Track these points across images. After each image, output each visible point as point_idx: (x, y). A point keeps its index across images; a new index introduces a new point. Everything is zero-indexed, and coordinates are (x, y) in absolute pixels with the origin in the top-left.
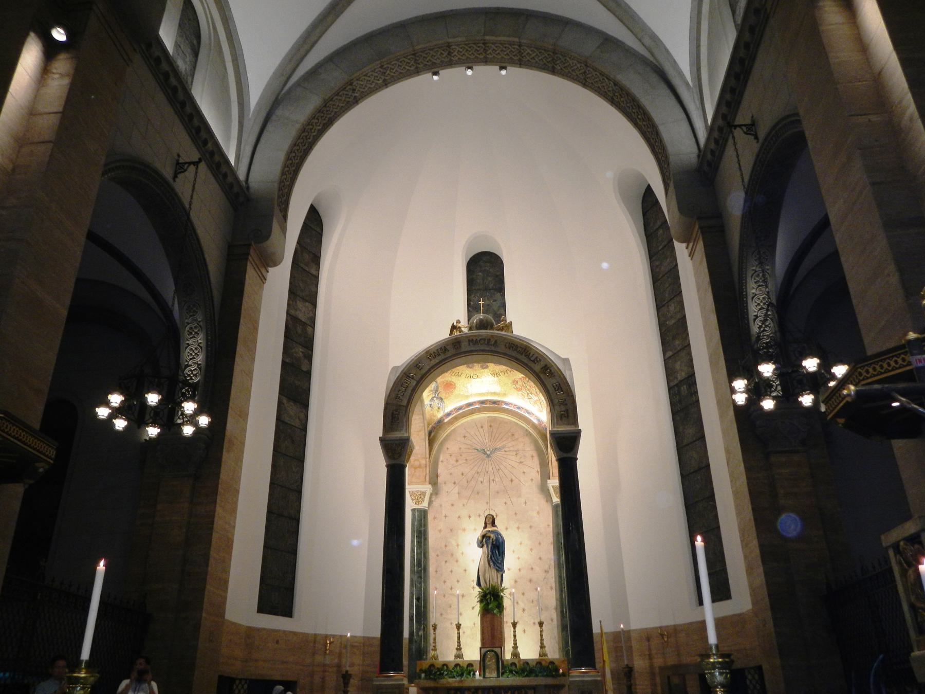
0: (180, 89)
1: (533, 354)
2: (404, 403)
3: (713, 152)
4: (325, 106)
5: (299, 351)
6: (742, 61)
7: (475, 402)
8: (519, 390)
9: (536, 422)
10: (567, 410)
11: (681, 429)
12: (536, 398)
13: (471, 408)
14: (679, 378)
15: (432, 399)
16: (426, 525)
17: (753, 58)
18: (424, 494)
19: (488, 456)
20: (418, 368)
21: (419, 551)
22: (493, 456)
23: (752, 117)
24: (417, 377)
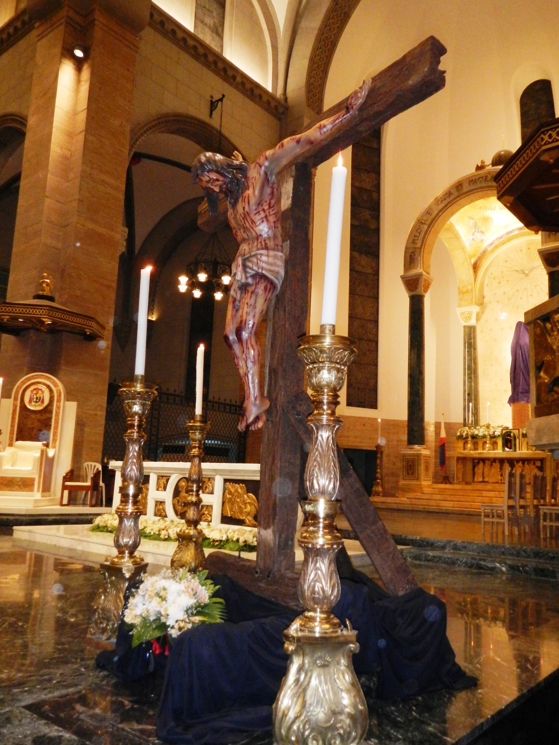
0: (199, 46)
2: (419, 245)
4: (337, 4)
5: (366, 214)
7: (514, 230)
13: (511, 235)
15: (473, 234)
16: (475, 338)
19: (527, 275)
21: (469, 358)
24: (428, 223)
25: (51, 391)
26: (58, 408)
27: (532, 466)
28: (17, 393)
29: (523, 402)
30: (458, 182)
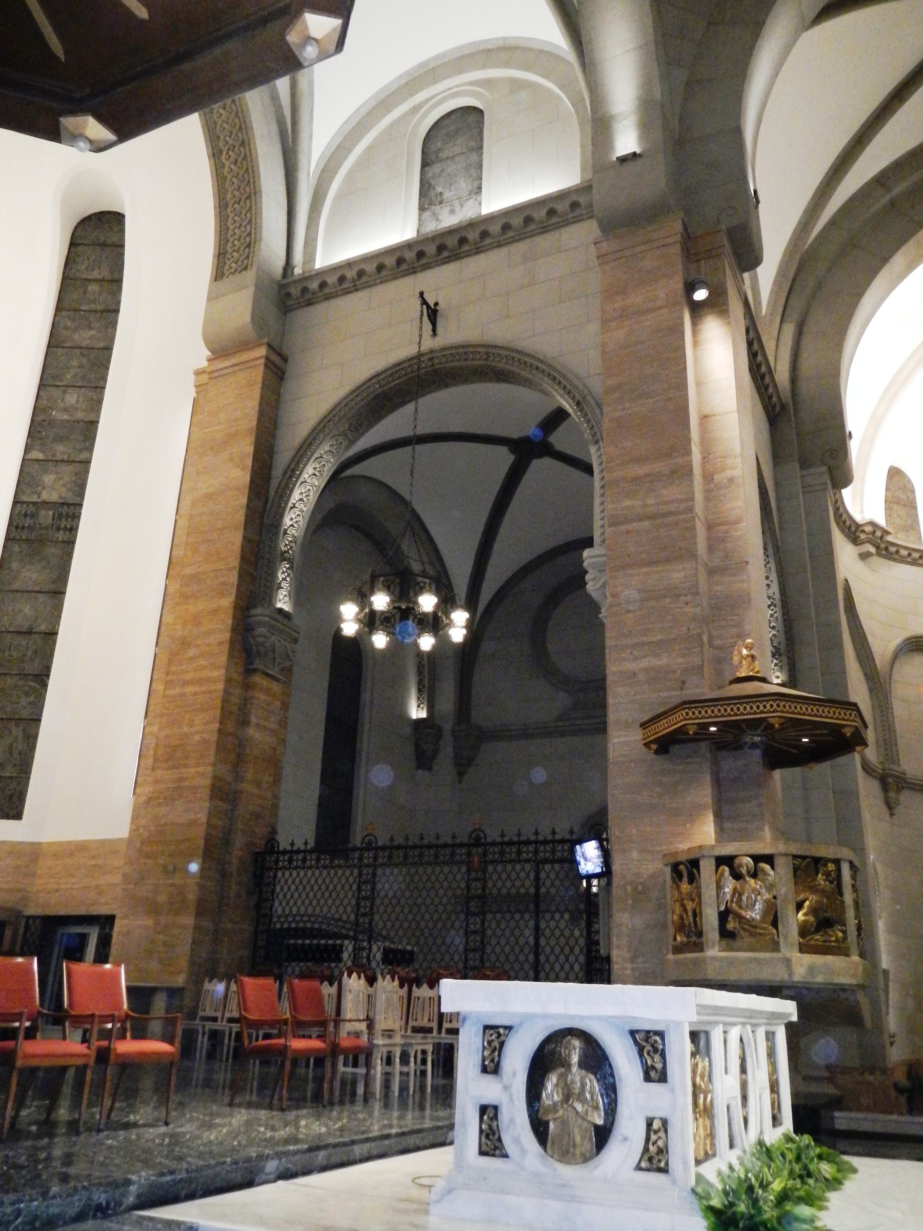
3: (323, 285)
6: (463, 241)
14: (45, 496)
17: (478, 251)
23: (436, 304)
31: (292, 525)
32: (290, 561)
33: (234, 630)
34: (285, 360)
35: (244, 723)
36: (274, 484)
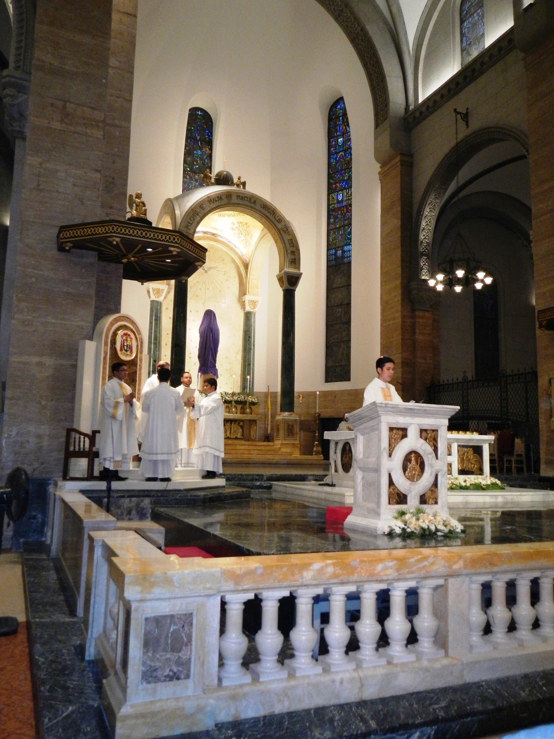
1: (278, 216)
3: (421, 113)
6: (474, 71)
8: (232, 229)
9: (239, 253)
10: (295, 259)
11: (332, 277)
12: (243, 238)
18: (163, 290)
19: (206, 272)
20: (202, 208)
22: (209, 272)
23: (467, 109)
24: (201, 215)
25: (136, 337)
26: (141, 360)
27: (236, 426)
28: (107, 337)
29: (211, 374)
30: (228, 192)
31: (425, 238)
32: (425, 255)
33: (403, 294)
34: (411, 156)
35: (414, 333)
36: (414, 220)
